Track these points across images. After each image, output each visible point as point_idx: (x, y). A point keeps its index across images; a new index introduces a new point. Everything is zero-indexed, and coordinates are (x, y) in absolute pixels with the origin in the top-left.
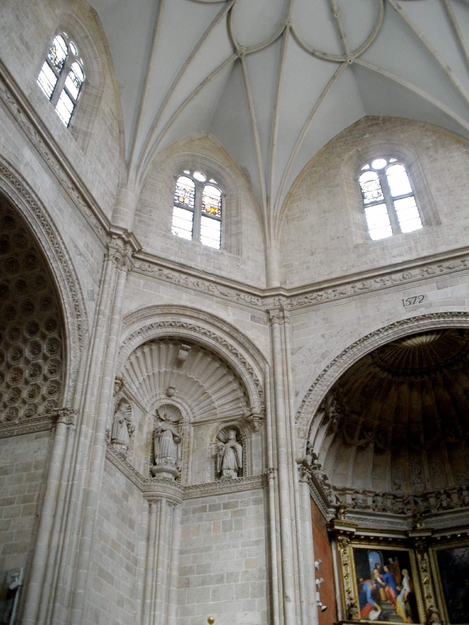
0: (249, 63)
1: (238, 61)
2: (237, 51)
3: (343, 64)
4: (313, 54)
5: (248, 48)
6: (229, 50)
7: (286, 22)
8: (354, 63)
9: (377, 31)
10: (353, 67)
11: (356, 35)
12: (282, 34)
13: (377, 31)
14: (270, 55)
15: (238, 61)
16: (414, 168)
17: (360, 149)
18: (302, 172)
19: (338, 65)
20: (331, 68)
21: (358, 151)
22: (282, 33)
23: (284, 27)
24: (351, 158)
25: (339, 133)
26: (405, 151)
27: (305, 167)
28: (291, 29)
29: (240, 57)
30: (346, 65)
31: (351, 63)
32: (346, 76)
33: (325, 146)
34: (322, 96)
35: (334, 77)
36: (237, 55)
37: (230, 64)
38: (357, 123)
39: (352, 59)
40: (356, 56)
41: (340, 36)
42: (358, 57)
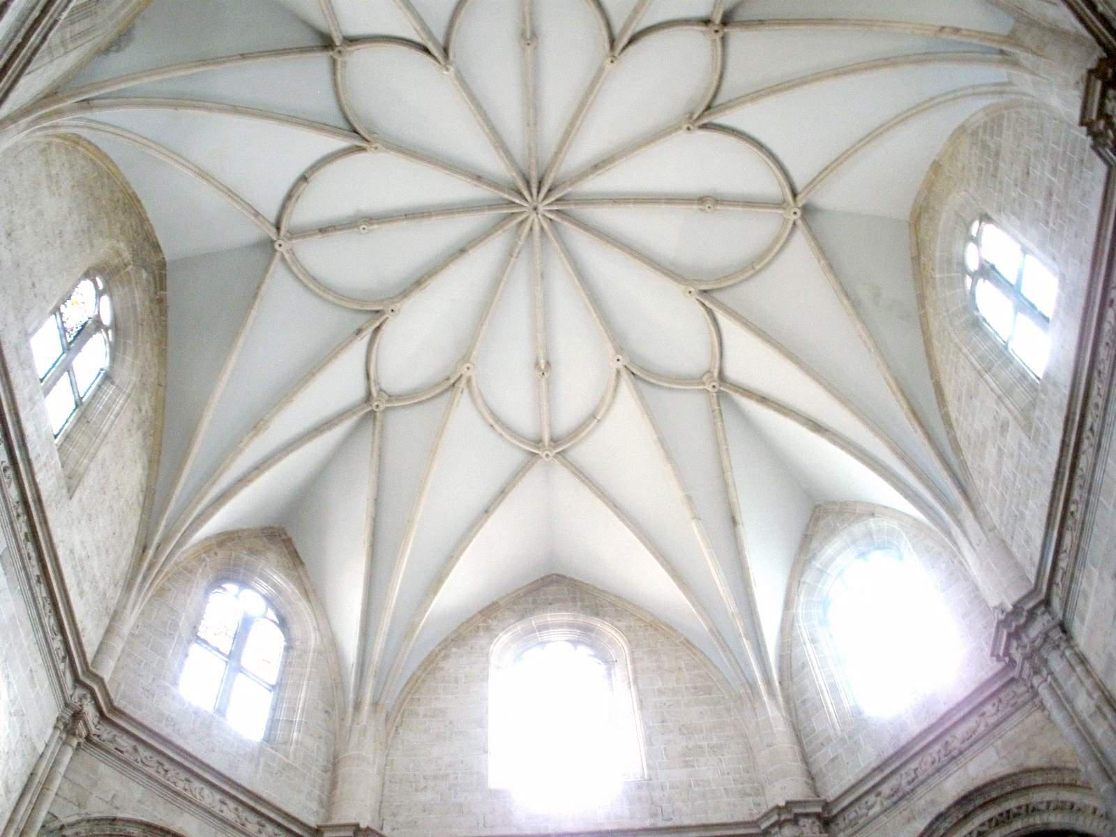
0: (320, 60)
1: (327, 43)
2: (349, 46)
3: (274, 230)
4: (304, 178)
5: (344, 64)
6: (353, 31)
7: (377, 145)
8: (275, 251)
9: (325, 296)
10: (268, 247)
11: (320, 257)
12: (355, 131)
13: (325, 296)
14: (320, 101)
15: (327, 43)
16: (110, 390)
17: (130, 267)
18: (105, 157)
19: (272, 219)
20: (271, 211)
21: (126, 265)
22: (357, 134)
23: (367, 137)
24: (118, 254)
25: (149, 215)
26: (129, 359)
27: (112, 161)
28: (360, 149)
29: (337, 49)
30: (274, 238)
31: (276, 246)
32: (249, 232)
33: (134, 193)
34: (231, 193)
35: (257, 214)
36: (341, 46)
37: (321, 23)
38: (156, 247)
39: (283, 248)
40: (287, 256)
41: (325, 230)
42: (283, 259)
